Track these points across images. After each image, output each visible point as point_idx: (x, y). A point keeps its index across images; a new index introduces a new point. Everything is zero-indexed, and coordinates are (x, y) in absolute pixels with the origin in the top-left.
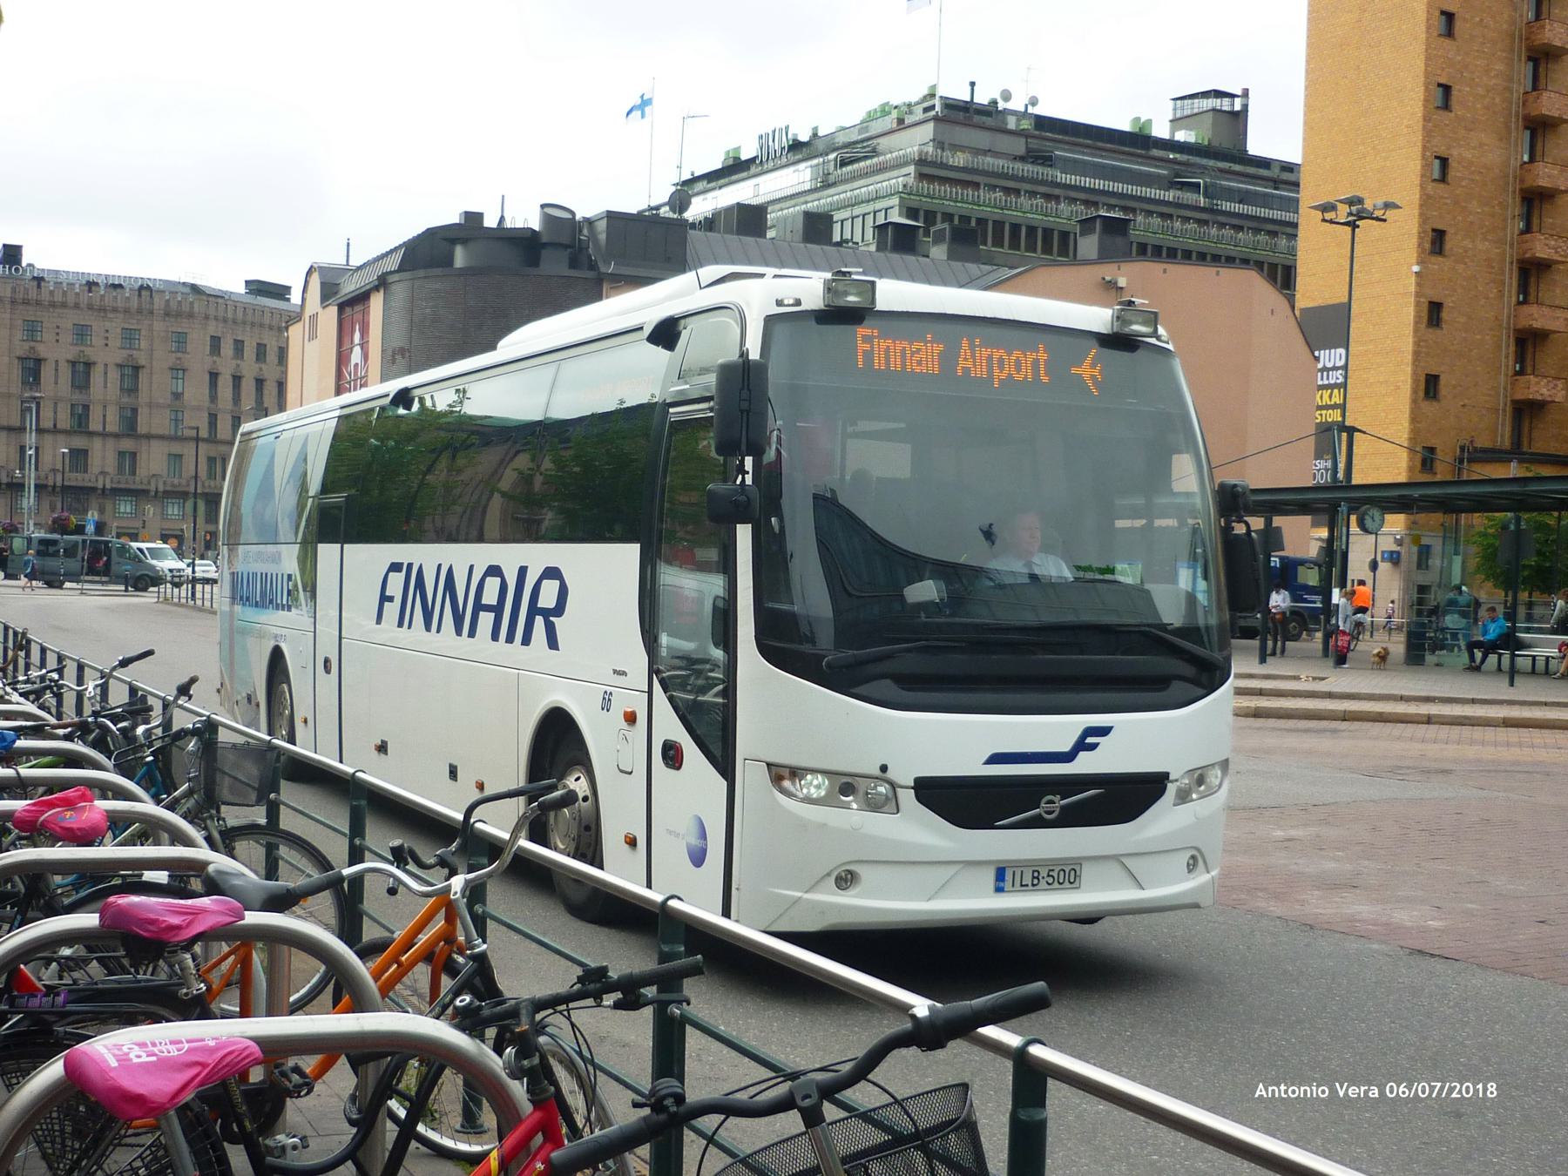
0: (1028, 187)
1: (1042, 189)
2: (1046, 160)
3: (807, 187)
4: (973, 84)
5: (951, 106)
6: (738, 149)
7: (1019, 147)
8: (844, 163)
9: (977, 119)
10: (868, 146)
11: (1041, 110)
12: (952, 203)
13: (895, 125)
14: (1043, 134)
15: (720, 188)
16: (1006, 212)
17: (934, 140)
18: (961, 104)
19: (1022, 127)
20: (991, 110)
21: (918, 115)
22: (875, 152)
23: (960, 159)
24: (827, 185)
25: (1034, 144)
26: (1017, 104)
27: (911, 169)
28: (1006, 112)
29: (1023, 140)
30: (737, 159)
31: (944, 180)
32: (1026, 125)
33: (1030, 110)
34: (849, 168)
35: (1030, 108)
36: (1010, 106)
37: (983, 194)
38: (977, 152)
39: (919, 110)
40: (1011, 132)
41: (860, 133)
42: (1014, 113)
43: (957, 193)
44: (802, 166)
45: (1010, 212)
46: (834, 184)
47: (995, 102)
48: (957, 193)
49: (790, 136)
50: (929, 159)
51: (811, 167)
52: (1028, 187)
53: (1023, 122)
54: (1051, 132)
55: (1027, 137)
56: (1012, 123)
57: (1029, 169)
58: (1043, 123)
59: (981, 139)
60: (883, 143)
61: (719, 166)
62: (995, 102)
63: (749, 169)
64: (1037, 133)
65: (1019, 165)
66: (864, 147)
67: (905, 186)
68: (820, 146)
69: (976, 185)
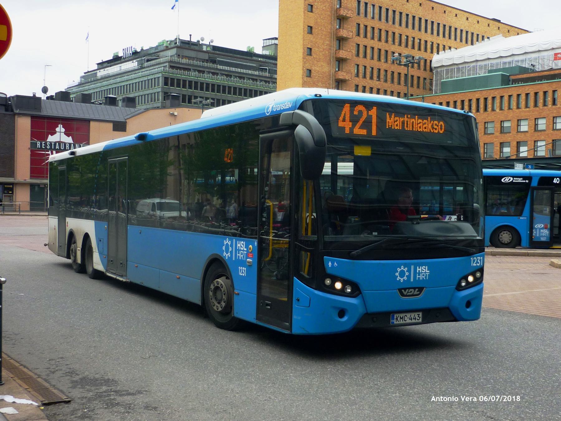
0: (207, 70)
1: (212, 71)
2: (214, 62)
3: (136, 68)
4: (190, 35)
5: (183, 42)
6: (117, 53)
7: (206, 57)
8: (148, 61)
9: (193, 47)
10: (157, 55)
11: (214, 44)
12: (180, 76)
13: (165, 48)
14: (215, 52)
15: (111, 66)
16: (199, 78)
17: (176, 54)
18: (187, 42)
19: (207, 50)
20: (197, 44)
21: (173, 45)
22: (158, 57)
23: (184, 61)
24: (142, 68)
25: (211, 55)
26: (206, 42)
27: (167, 64)
28: (202, 45)
29: (207, 54)
30: (117, 56)
31: (180, 68)
32: (209, 49)
33: (211, 44)
34: (149, 62)
35: (211, 43)
36: (204, 42)
37: (193, 73)
38: (189, 58)
39: (173, 43)
40: (204, 52)
41: (155, 50)
42: (205, 45)
43: (182, 72)
44: (135, 61)
45: (200, 79)
46: (144, 68)
47: (199, 41)
48: (182, 72)
49: (133, 50)
50: (173, 61)
51: (137, 61)
52: (207, 70)
53: (208, 48)
54: (218, 51)
55: (209, 53)
56: (204, 49)
57: (210, 65)
58: (215, 48)
59: (192, 54)
60: (161, 54)
61: (112, 58)
62: (199, 41)
63: (121, 60)
64: (213, 51)
65: (205, 64)
66: (155, 55)
67: (164, 70)
68: (143, 53)
69: (189, 70)
